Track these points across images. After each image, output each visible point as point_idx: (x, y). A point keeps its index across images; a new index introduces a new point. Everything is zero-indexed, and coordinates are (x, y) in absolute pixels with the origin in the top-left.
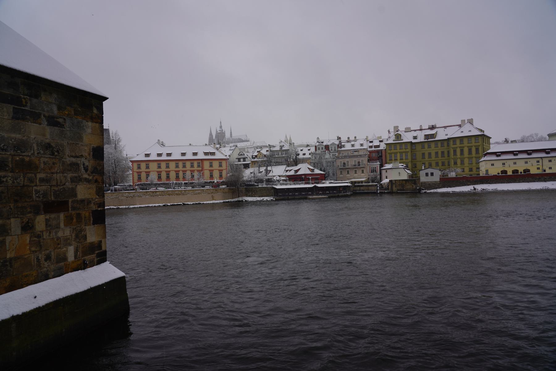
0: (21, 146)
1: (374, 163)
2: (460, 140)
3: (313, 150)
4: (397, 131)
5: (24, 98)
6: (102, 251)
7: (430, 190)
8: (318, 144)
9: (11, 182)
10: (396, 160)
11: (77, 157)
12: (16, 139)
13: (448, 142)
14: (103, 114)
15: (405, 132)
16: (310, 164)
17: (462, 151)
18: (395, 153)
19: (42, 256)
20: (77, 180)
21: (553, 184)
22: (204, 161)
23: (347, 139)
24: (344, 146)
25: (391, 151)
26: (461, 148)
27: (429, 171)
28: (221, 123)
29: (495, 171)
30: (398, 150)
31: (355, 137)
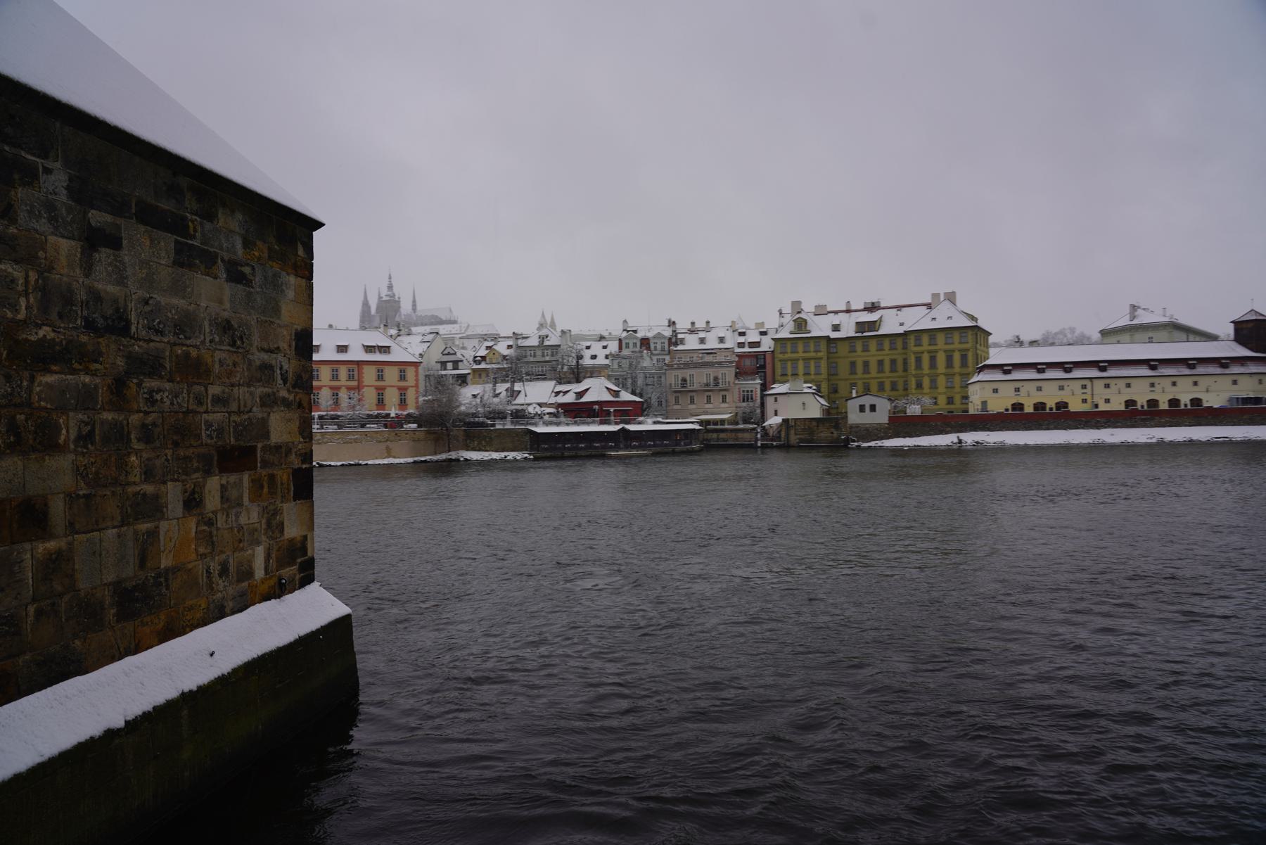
0: (185, 325)
1: (748, 380)
2: (930, 336)
3: (613, 347)
4: (799, 312)
5: (192, 221)
6: (306, 558)
7: (867, 442)
8: (625, 334)
9: (168, 403)
10: (795, 375)
11: (271, 352)
12: (179, 310)
13: (905, 341)
14: (312, 258)
15: (816, 315)
16: (609, 377)
17: (933, 359)
18: (795, 360)
19: (215, 567)
20: (269, 402)
21: (1112, 435)
22: (364, 366)
23: (689, 326)
24: (682, 341)
25: (786, 356)
26: (949, 354)
27: (867, 400)
28: (390, 278)
29: (999, 405)
30: (801, 354)
31: (708, 322)
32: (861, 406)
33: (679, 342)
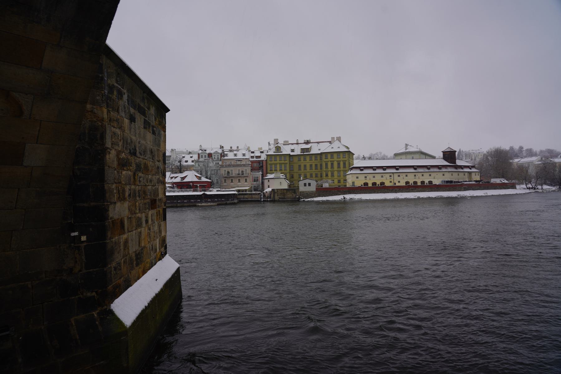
1: (255, 172)
2: (331, 154)
3: (195, 157)
4: (277, 144)
7: (307, 199)
8: (200, 151)
13: (321, 157)
14: (166, 124)
15: (284, 145)
16: (197, 171)
17: (332, 164)
21: (401, 195)
23: (229, 148)
24: (227, 155)
27: (307, 181)
29: (359, 183)
30: (278, 162)
31: (238, 147)
32: (304, 183)
33: (225, 155)
